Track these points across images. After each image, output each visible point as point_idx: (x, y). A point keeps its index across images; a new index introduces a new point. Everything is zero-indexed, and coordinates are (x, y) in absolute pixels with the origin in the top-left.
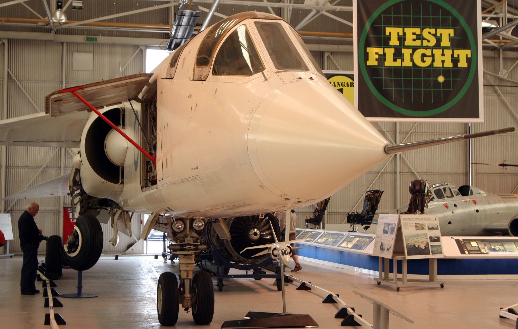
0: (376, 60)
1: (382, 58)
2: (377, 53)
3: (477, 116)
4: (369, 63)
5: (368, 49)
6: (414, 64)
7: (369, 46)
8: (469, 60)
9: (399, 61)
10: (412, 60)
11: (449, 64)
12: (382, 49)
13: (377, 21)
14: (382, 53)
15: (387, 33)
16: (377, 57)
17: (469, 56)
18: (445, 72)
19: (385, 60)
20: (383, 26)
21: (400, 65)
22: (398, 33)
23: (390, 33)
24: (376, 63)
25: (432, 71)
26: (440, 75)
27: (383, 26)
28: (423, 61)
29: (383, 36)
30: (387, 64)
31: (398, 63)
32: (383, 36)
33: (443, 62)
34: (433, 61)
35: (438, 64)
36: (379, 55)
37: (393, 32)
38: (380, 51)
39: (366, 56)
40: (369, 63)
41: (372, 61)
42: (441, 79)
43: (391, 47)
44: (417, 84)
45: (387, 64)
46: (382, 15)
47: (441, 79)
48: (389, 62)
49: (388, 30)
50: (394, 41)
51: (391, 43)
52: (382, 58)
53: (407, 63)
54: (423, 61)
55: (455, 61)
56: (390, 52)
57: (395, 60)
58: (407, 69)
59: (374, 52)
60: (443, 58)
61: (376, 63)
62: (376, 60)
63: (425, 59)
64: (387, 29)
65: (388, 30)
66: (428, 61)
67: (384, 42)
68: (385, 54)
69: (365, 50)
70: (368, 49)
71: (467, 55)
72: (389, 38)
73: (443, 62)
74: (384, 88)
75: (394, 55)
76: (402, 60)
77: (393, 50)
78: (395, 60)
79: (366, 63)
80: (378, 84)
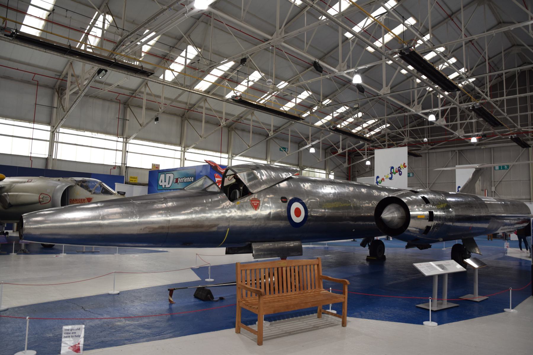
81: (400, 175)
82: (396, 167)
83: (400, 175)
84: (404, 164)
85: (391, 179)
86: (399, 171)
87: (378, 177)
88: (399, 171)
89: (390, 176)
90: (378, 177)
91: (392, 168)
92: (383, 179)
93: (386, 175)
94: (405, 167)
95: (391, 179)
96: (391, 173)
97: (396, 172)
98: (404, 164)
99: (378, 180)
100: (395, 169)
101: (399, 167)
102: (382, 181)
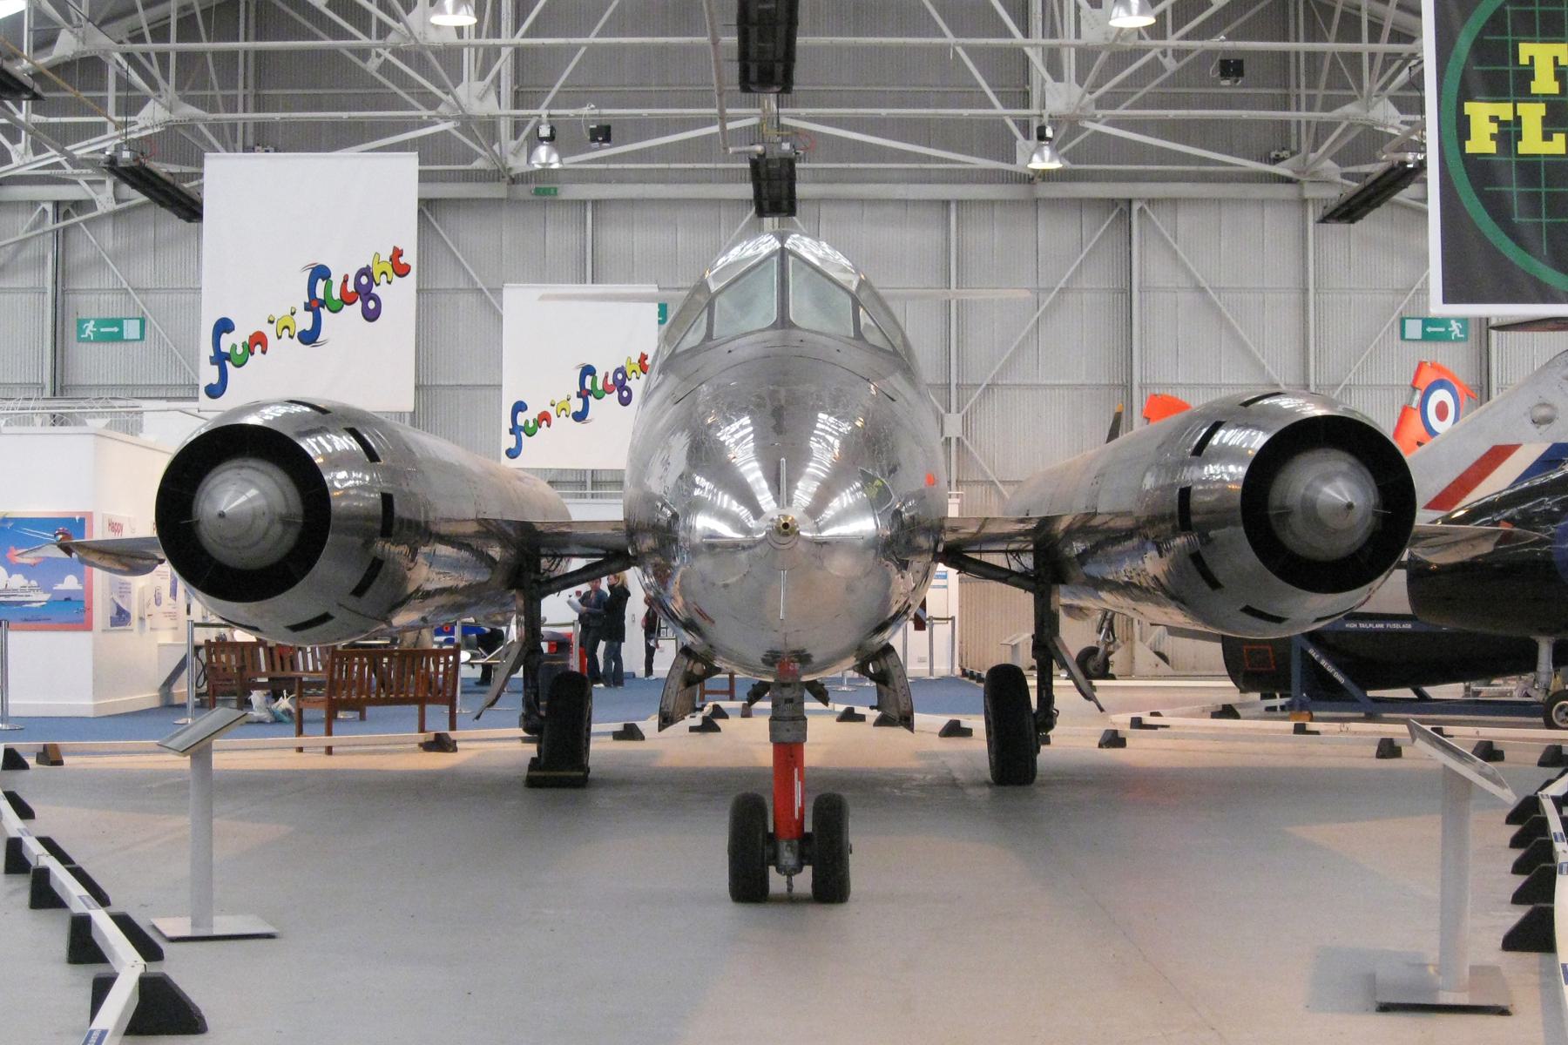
0: (1493, 137)
1: (1509, 133)
2: (1494, 119)
4: (1471, 147)
5: (1470, 108)
7: (1471, 100)
12: (1510, 106)
13: (1496, 22)
14: (1510, 117)
15: (1524, 60)
16: (1494, 128)
19: (1519, 137)
20: (1510, 38)
22: (1556, 59)
23: (1531, 58)
24: (1491, 147)
27: (1510, 38)
29: (1510, 68)
30: (1524, 148)
32: (1510, 68)
36: (1502, 124)
37: (1542, 58)
38: (1505, 111)
39: (1463, 128)
40: (1471, 147)
41: (1481, 142)
43: (1535, 99)
45: (1524, 148)
46: (1508, 8)
48: (1532, 142)
49: (1526, 50)
50: (1545, 83)
51: (1536, 87)
52: (1509, 133)
56: (1532, 114)
57: (1547, 137)
59: (1482, 116)
61: (1491, 147)
62: (1493, 137)
64: (1522, 46)
65: (1526, 50)
67: (1517, 84)
68: (1518, 120)
69: (1460, 108)
70: (1470, 108)
72: (1528, 74)
75: (1546, 121)
77: (1540, 109)
78: (1547, 137)
79: (1462, 147)
80: (1497, 208)
81: (371, 316)
82: (343, 268)
83: (371, 316)
84: (398, 253)
87: (224, 326)
88: (363, 294)
89: (305, 321)
90: (224, 326)
91: (320, 273)
92: (258, 340)
93: (280, 312)
94: (402, 271)
96: (314, 306)
97: (347, 299)
98: (398, 253)
99: (226, 342)
101: (365, 271)
102: (249, 349)
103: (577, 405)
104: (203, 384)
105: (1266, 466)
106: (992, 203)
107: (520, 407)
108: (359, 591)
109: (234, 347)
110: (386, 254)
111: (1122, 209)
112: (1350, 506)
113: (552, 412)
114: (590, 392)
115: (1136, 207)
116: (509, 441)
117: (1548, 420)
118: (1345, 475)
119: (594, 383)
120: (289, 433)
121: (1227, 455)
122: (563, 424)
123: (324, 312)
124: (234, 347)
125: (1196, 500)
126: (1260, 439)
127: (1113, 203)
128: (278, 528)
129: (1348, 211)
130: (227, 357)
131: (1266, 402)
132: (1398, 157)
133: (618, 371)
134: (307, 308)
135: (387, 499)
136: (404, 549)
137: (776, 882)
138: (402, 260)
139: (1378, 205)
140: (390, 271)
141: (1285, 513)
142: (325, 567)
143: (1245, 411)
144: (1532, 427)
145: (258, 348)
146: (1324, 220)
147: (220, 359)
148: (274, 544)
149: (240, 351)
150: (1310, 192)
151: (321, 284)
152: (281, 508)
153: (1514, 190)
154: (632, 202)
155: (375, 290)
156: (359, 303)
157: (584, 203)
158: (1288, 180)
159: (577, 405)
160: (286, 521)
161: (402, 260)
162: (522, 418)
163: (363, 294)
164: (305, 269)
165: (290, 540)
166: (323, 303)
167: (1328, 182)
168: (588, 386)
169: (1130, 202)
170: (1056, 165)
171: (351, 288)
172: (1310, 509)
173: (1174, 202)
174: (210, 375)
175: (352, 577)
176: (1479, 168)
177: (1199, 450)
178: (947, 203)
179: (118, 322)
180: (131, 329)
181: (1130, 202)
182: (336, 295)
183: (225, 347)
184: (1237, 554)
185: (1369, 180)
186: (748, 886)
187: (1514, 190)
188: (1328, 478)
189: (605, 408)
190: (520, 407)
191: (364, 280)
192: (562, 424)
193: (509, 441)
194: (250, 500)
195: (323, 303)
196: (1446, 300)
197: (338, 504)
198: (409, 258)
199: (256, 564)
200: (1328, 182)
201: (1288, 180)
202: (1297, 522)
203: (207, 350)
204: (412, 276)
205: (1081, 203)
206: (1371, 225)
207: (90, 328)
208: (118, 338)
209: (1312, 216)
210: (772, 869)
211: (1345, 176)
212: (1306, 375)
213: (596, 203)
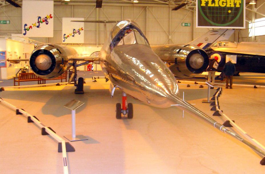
0: (205, 4)
3: (242, 26)
6: (219, 6)
8: (240, 4)
9: (213, 4)
10: (219, 4)
11: (233, 6)
16: (205, 2)
17: (240, 3)
18: (231, 8)
19: (208, 4)
21: (214, 6)
25: (225, 8)
26: (229, 10)
28: (223, 5)
31: (213, 5)
33: (230, 5)
34: (227, 4)
35: (228, 6)
36: (206, 2)
42: (230, 11)
44: (221, 13)
47: (230, 11)
53: (217, 5)
54: (223, 5)
55: (235, 4)
57: (212, 4)
58: (217, 7)
60: (230, 3)
62: (205, 4)
63: (224, 3)
66: (225, 4)
71: (239, 2)
73: (230, 5)
74: (208, 15)
76: (215, 4)
78: (212, 4)
79: (201, 5)
80: (205, 13)
81: (47, 24)
83: (47, 24)
84: (51, 15)
85: (38, 27)
86: (46, 20)
87: (26, 25)
88: (46, 21)
89: (37, 24)
90: (26, 25)
92: (31, 27)
94: (51, 17)
95: (38, 27)
96: (39, 22)
97: (43, 21)
98: (51, 15)
99: (26, 27)
100: (42, 18)
103: (73, 34)
104: (23, 33)
105: (189, 56)
106: (127, 6)
107: (65, 35)
108: (59, 73)
109: (27, 28)
110: (49, 15)
111: (145, 8)
112: (202, 62)
113: (69, 35)
114: (74, 33)
115: (147, 7)
116: (63, 39)
117: (207, 40)
118: (200, 58)
119: (75, 31)
120: (48, 50)
121: (183, 53)
122: (71, 37)
123: (40, 23)
124: (27, 28)
125: (178, 59)
126: (188, 52)
127: (144, 7)
128: (48, 65)
129: (176, 9)
130: (26, 29)
131: (188, 46)
132: (184, 2)
133: (79, 30)
134: (38, 22)
135: (63, 59)
136: (63, 65)
137: (122, 115)
138: (51, 16)
139: (180, 8)
140: (49, 17)
141: (192, 62)
142: (55, 70)
143: (185, 48)
144: (205, 41)
145: (31, 28)
146: (173, 10)
147: (25, 30)
148: (47, 67)
149: (28, 29)
150: (170, 6)
151: (40, 19)
152: (49, 62)
153: (207, 11)
154: (78, 5)
155: (47, 20)
156: (45, 22)
157: (72, 5)
158: (167, 4)
159: (73, 34)
160: (49, 63)
161: (51, 16)
162: (65, 36)
163: (46, 21)
164: (37, 17)
165: (50, 65)
166: (40, 22)
167: (173, 5)
168: (74, 32)
169: (146, 7)
170: (138, 2)
171: (44, 20)
172: (196, 62)
173: (152, 7)
174: (24, 32)
175: (58, 71)
176: (202, 7)
177: (178, 53)
178: (122, 6)
179: (6, 21)
180: (8, 22)
181: (146, 7)
182: (42, 21)
183: (26, 28)
184: (184, 67)
185: (180, 5)
186: (119, 116)
187: (207, 11)
188: (198, 58)
189: (77, 35)
190: (65, 35)
191: (46, 19)
192: (71, 37)
193: (63, 39)
194: (44, 61)
195: (40, 22)
196: (198, 26)
197: (57, 60)
198: (52, 16)
199: (45, 70)
200: (173, 5)
201: (167, 4)
202: (194, 64)
203: (23, 29)
204: (53, 18)
205: (140, 7)
206: (179, 11)
207: (2, 22)
208: (6, 23)
209: (171, 9)
210: (122, 114)
211: (175, 4)
212: (169, 30)
213: (73, 5)
